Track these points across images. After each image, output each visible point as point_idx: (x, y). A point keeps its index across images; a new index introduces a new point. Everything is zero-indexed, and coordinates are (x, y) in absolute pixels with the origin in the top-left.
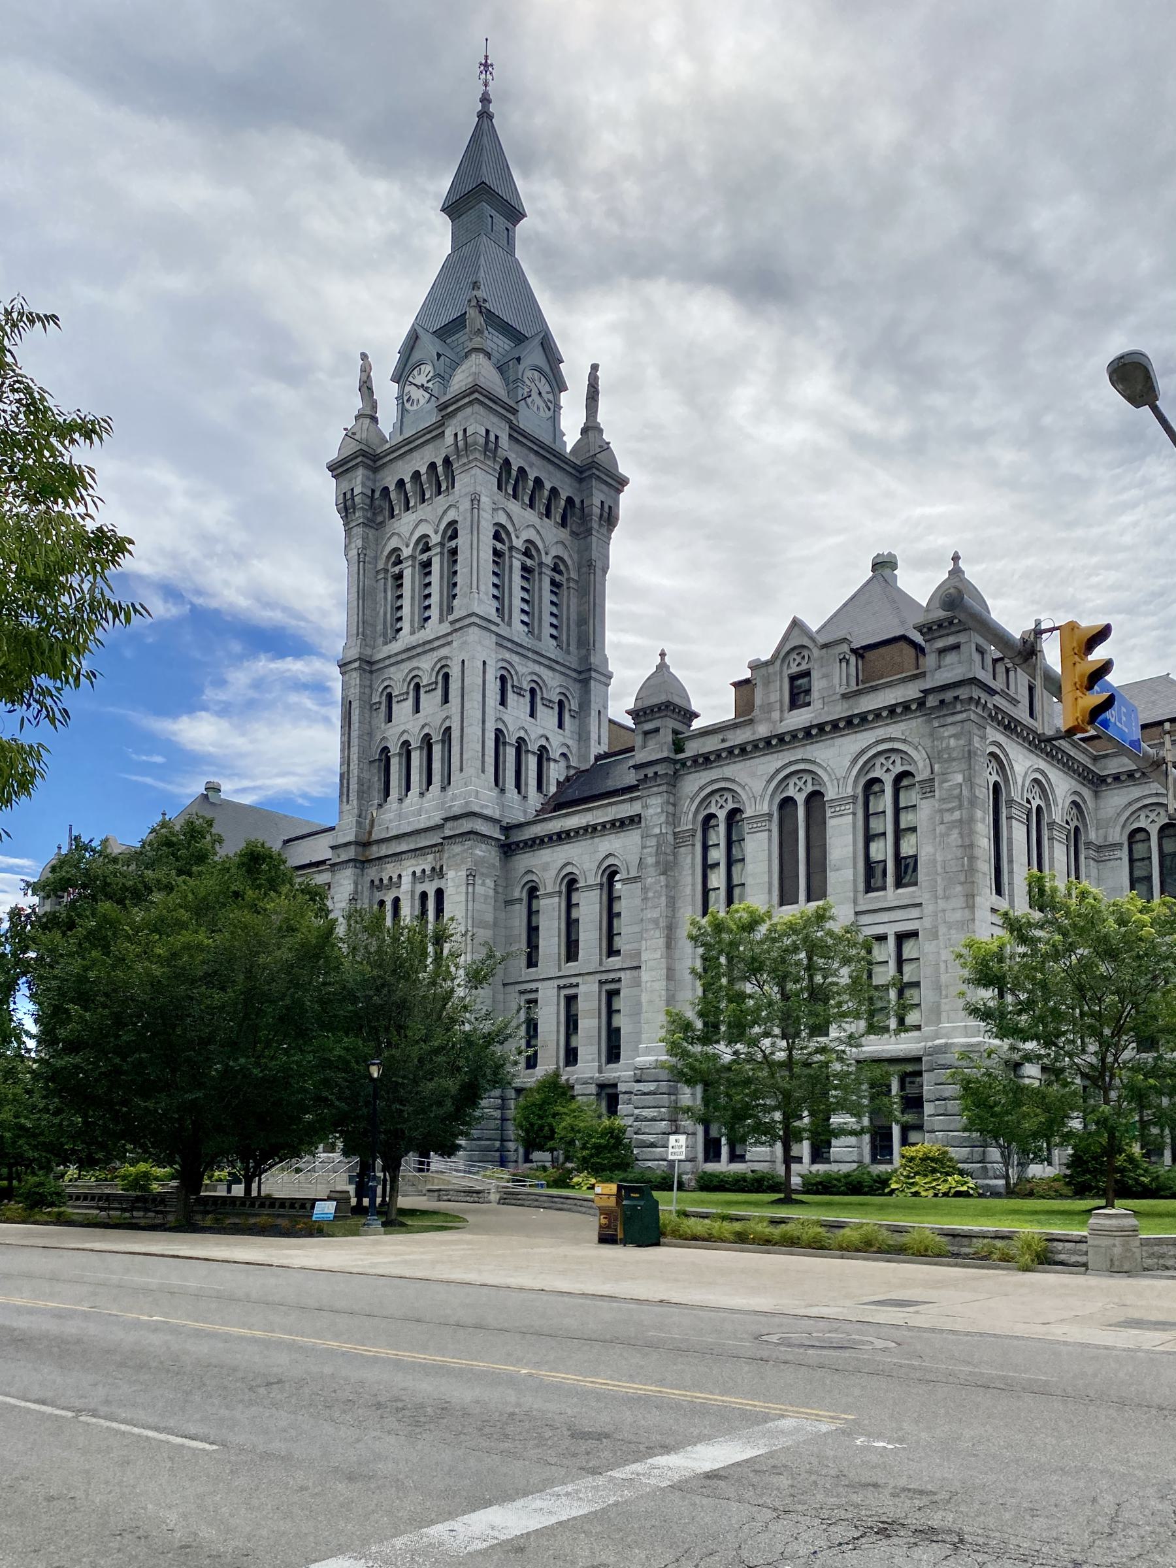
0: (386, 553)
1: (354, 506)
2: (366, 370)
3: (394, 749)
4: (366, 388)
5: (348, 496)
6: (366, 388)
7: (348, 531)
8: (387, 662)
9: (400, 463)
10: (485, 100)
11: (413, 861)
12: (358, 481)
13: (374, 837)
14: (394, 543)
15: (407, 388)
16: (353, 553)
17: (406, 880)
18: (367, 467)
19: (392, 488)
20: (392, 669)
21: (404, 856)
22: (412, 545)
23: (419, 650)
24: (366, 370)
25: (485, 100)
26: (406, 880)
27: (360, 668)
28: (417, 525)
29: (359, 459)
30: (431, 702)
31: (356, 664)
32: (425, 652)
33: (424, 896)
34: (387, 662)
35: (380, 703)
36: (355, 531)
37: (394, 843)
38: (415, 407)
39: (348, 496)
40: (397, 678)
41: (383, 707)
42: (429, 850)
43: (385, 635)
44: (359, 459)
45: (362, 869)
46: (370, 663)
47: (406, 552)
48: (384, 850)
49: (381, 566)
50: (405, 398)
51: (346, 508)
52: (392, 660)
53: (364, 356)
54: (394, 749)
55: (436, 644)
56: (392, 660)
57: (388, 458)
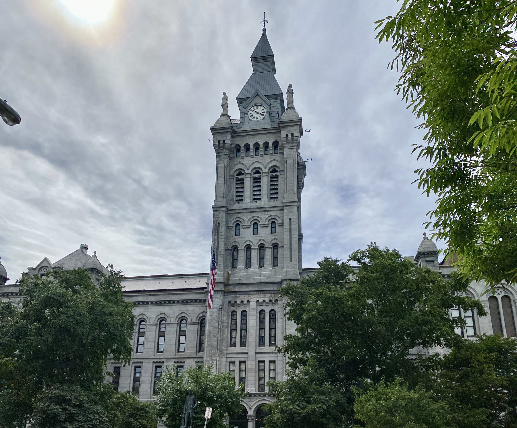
0: (235, 169)
1: (224, 147)
2: (225, 98)
3: (242, 246)
4: (225, 105)
5: (222, 142)
6: (225, 105)
7: (218, 156)
8: (237, 211)
9: (247, 137)
10: (264, 30)
11: (254, 296)
12: (228, 139)
13: (230, 282)
15: (250, 112)
16: (222, 165)
17: (253, 303)
18: (231, 134)
19: (242, 145)
20: (240, 215)
21: (251, 293)
22: (250, 170)
23: (248, 211)
24: (225, 98)
25: (264, 30)
26: (253, 303)
27: (225, 210)
28: (254, 163)
29: (229, 130)
31: (224, 209)
32: (260, 211)
33: (262, 312)
34: (237, 211)
35: (250, 225)
36: (222, 157)
37: (244, 286)
38: (255, 119)
39: (222, 142)
40: (246, 219)
41: (234, 229)
42: (268, 292)
43: (233, 201)
44: (229, 130)
45: (224, 295)
46: (228, 210)
47: (247, 172)
48: (237, 289)
49: (232, 173)
50: (249, 115)
51: (219, 147)
53: (224, 94)
54: (242, 246)
55: (268, 209)
57: (241, 134)
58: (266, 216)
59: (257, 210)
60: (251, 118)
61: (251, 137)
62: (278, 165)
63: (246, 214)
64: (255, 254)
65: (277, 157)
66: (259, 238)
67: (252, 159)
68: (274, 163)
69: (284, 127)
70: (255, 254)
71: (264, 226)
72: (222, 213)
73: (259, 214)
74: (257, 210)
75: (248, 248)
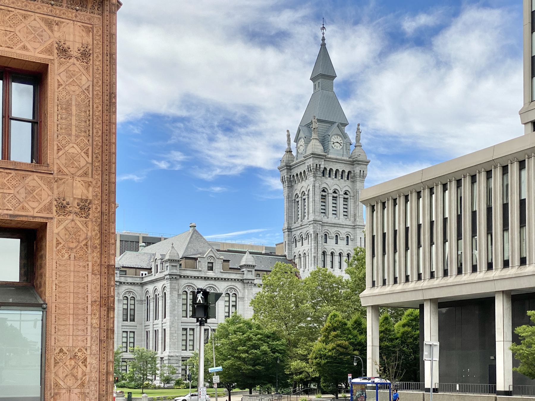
14: (325, 186)
30: (342, 243)
38: (336, 148)
40: (332, 231)
52: (327, 224)
56: (327, 224)
58: (344, 232)
59: (338, 226)
60: (333, 146)
61: (334, 163)
62: (349, 190)
63: (331, 228)
64: (337, 259)
65: (348, 183)
66: (339, 248)
67: (332, 181)
68: (347, 188)
69: (359, 164)
70: (337, 259)
71: (342, 239)
72: (319, 225)
73: (339, 229)
74: (338, 226)
75: (332, 254)
